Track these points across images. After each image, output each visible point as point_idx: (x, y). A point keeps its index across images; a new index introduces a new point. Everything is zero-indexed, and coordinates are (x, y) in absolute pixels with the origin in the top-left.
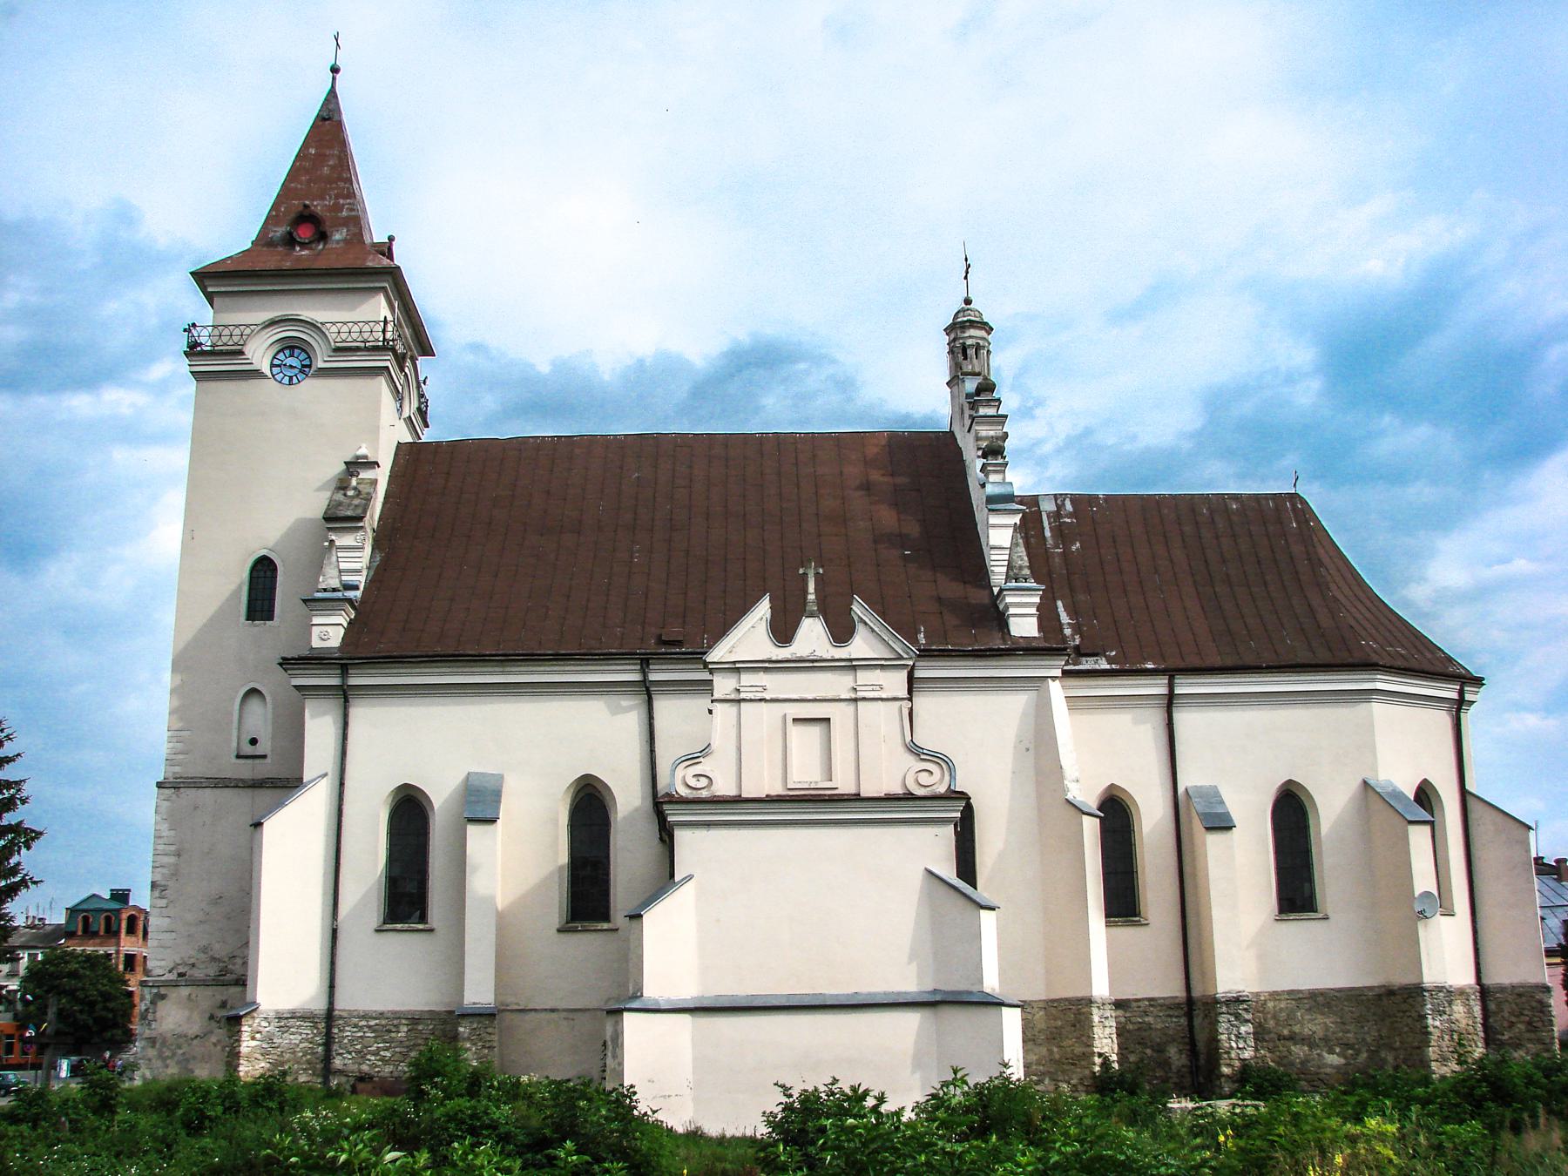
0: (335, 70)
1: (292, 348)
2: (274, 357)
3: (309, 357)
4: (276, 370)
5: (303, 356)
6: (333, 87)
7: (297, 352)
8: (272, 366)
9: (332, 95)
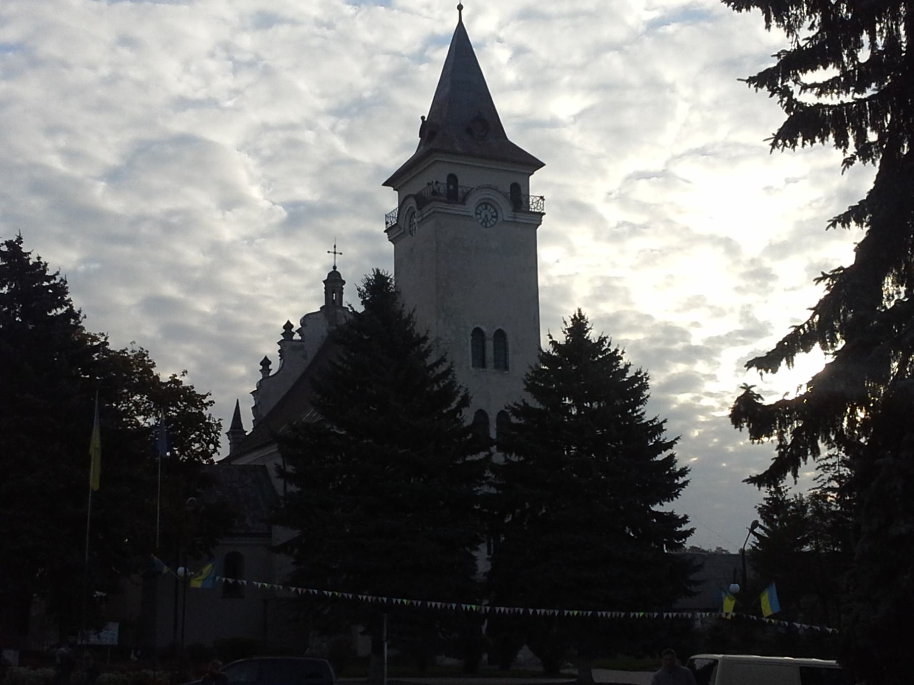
0: (460, 8)
2: (477, 209)
3: (496, 211)
4: (479, 217)
5: (492, 210)
7: (489, 207)
8: (476, 214)
9: (460, 23)
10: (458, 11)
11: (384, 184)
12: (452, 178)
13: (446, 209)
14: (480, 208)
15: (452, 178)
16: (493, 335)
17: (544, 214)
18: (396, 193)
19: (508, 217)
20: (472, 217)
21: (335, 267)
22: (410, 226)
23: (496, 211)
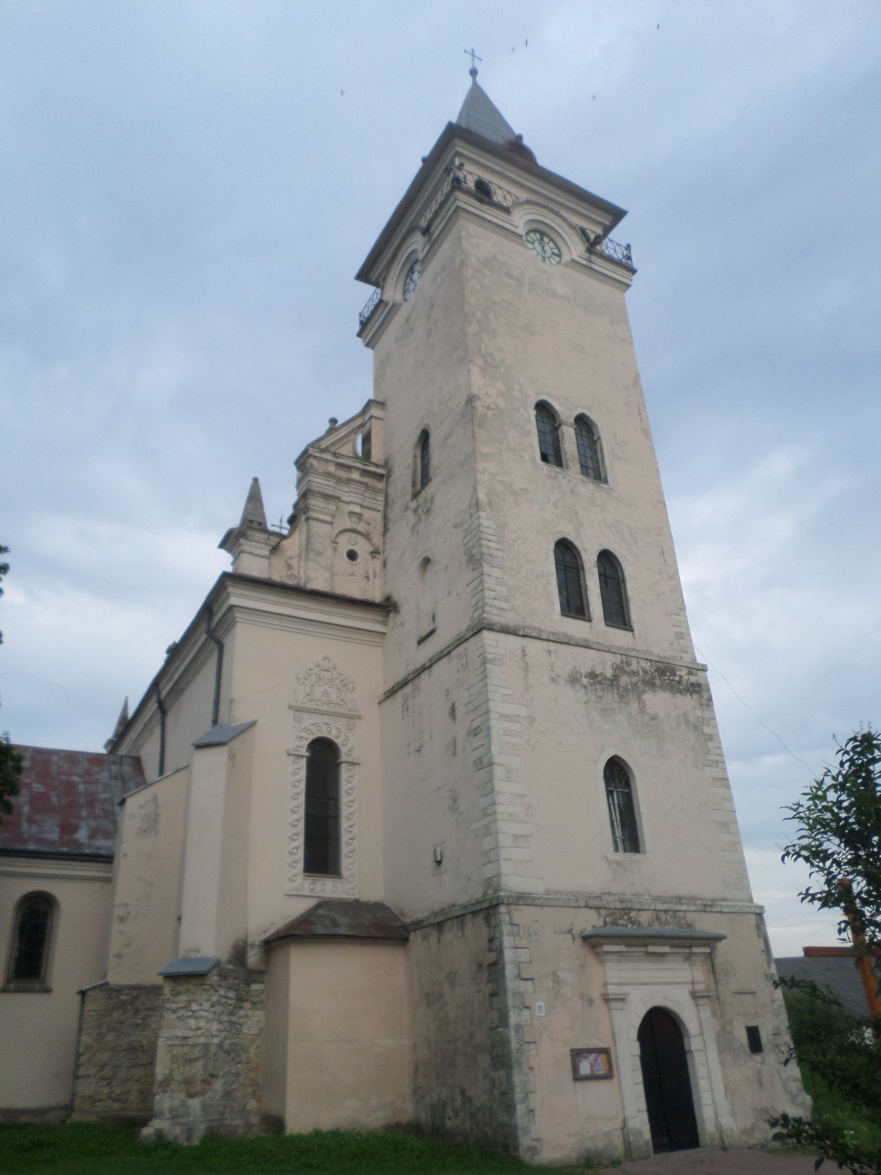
1: (542, 234)
3: (558, 248)
7: (546, 240)
13: (476, 208)
14: (532, 235)
16: (573, 420)
19: (579, 257)
20: (520, 236)
23: (558, 248)
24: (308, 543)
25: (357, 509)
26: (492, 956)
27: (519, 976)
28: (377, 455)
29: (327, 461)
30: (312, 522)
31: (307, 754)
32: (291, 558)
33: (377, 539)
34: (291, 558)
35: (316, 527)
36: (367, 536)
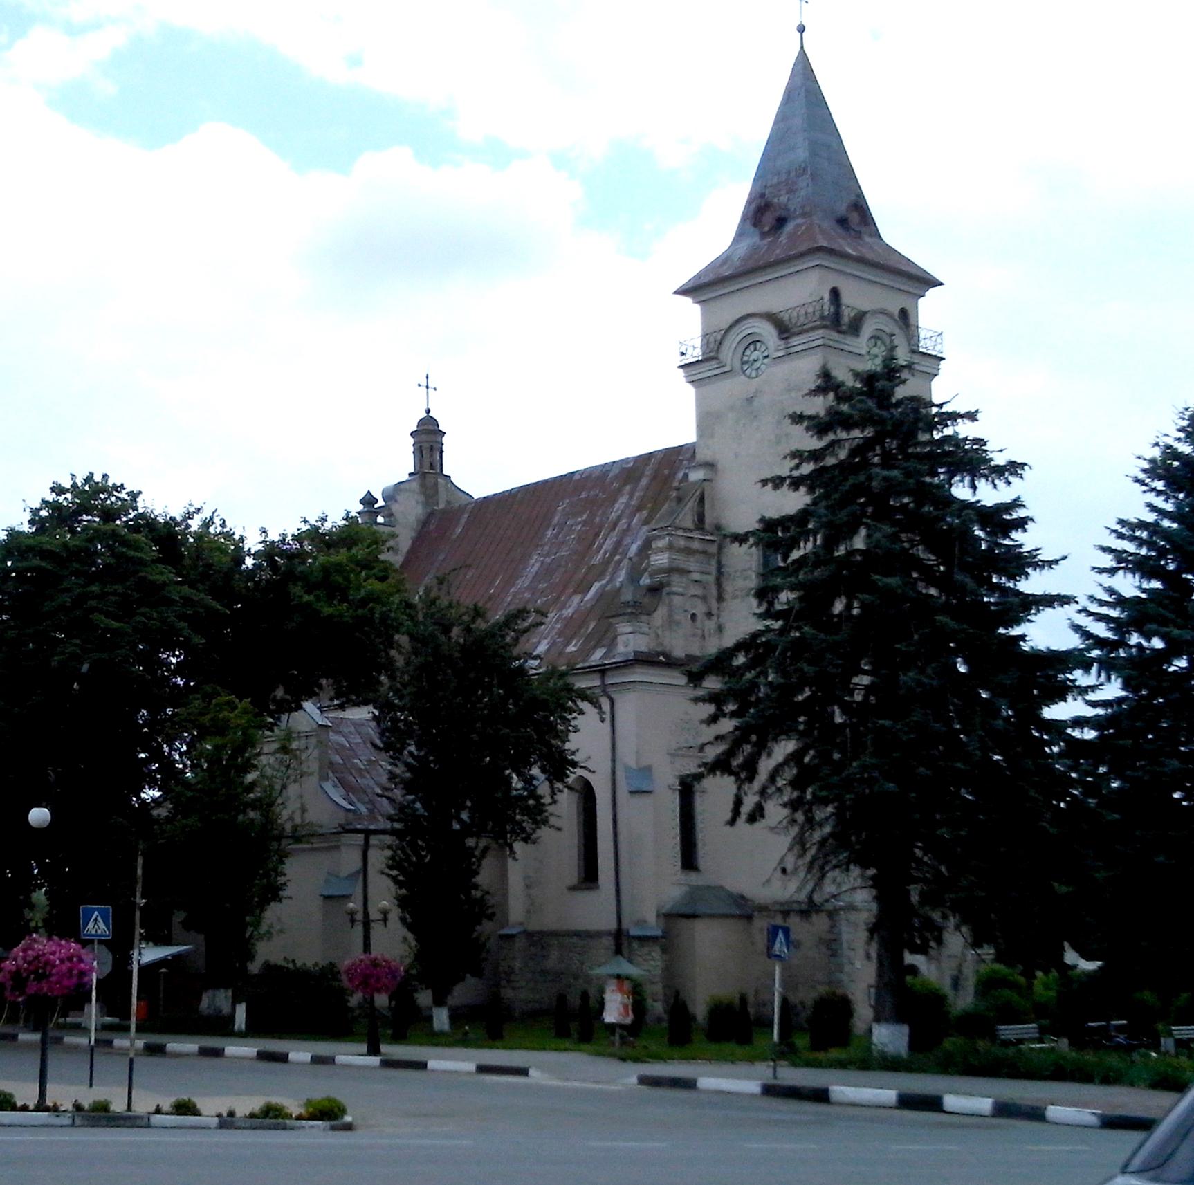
0: (801, 29)
6: (802, 47)
7: (879, 343)
10: (799, 34)
11: (676, 293)
12: (835, 293)
13: (837, 341)
15: (835, 293)
17: (942, 359)
18: (697, 308)
21: (428, 411)
22: (743, 363)
24: (670, 616)
25: (696, 576)
26: (833, 937)
27: (849, 948)
28: (709, 520)
29: (679, 536)
30: (672, 596)
31: (679, 788)
32: (658, 628)
33: (714, 604)
34: (658, 628)
35: (677, 600)
36: (704, 598)
